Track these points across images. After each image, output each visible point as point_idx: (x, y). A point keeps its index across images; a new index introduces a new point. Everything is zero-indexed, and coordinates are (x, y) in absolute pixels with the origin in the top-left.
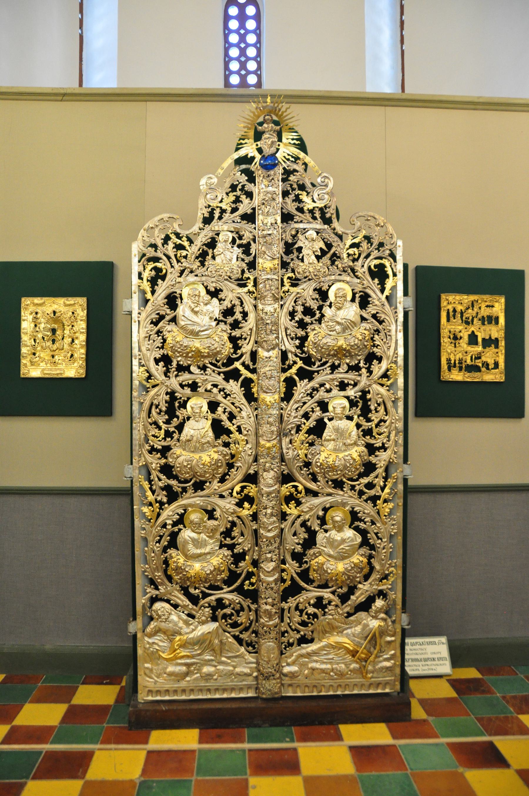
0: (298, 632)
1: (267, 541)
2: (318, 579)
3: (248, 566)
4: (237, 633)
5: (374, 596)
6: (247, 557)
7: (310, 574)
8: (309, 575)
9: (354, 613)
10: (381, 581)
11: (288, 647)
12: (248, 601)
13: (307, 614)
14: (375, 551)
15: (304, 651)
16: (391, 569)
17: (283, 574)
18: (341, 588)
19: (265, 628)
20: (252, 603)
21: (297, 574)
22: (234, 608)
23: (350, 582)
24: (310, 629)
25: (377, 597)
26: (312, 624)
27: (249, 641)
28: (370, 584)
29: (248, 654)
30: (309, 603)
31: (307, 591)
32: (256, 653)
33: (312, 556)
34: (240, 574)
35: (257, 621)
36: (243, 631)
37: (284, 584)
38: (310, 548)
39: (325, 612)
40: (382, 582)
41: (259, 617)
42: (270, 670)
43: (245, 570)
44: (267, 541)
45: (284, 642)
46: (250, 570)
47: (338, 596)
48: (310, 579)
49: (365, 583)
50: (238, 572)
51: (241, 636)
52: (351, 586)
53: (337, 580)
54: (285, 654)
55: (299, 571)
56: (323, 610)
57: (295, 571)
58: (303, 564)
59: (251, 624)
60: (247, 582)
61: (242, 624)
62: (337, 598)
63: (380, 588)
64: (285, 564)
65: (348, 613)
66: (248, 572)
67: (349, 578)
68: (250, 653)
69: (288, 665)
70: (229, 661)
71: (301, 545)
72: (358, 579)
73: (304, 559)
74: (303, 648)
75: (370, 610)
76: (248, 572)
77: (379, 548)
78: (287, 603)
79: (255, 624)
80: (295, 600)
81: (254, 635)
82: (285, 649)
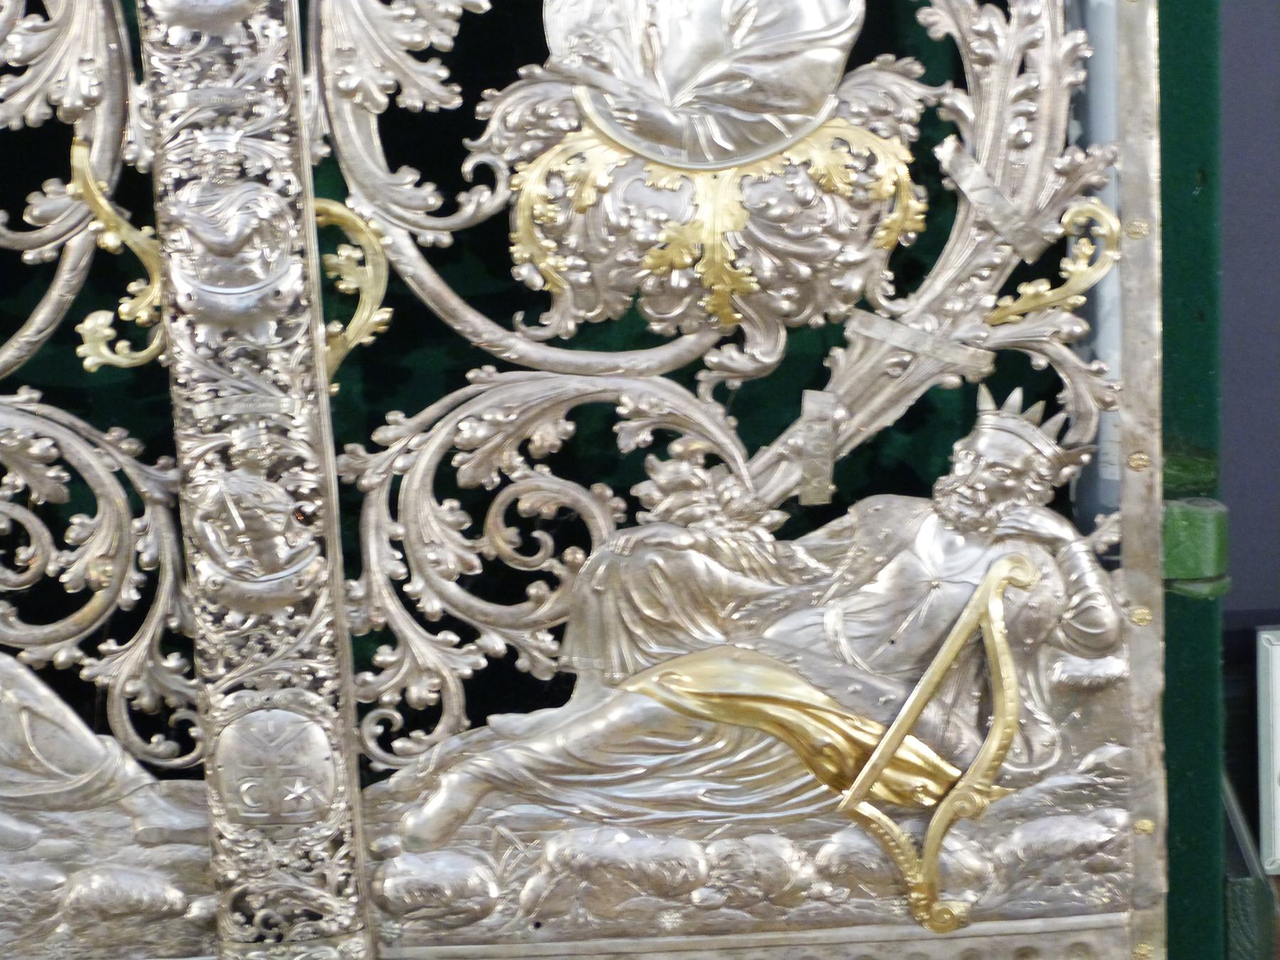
0: (468, 634)
1: (196, 38)
2: (576, 286)
3: (92, 215)
4: (63, 655)
5: (968, 391)
6: (80, 157)
7: (517, 251)
8: (509, 262)
9: (836, 508)
10: (1009, 289)
11: (404, 733)
12: (115, 444)
13: (512, 516)
14: (961, 83)
15: (516, 757)
16: (1078, 210)
17: (331, 259)
18: (738, 338)
19: (232, 618)
20: (147, 458)
21: (431, 254)
22: (27, 491)
23: (801, 302)
24: (544, 610)
25: (985, 400)
26: (553, 581)
27: (145, 701)
28: (936, 309)
29: (147, 778)
30: (524, 448)
31: (505, 366)
32: (196, 772)
33: (521, 129)
34: (48, 271)
35: (184, 572)
36: (99, 636)
37: (346, 321)
38: (504, 79)
39: (635, 505)
40: (1017, 296)
41: (190, 551)
42: (291, 882)
43: (76, 243)
44: (196, 38)
45: (376, 704)
46: (110, 241)
47: (720, 393)
48: (522, 287)
49: (899, 306)
50: (29, 256)
51: (91, 669)
52: (805, 326)
53: (697, 286)
54: (388, 774)
55: (446, 239)
56: (622, 491)
57: (414, 237)
58: (467, 187)
59: (149, 589)
60: (97, 324)
61: (86, 594)
62: (719, 410)
63: (1002, 336)
64: (341, 193)
65: (788, 503)
66: (100, 257)
67: (785, 276)
68: (160, 773)
69: (415, 844)
70: (35, 831)
71: (446, 58)
72: (854, 282)
73: (465, 153)
74: (500, 735)
75: (943, 482)
76: (100, 257)
77: (986, 61)
78: (374, 448)
79: (176, 593)
80: (427, 428)
81: (173, 661)
82: (385, 742)
